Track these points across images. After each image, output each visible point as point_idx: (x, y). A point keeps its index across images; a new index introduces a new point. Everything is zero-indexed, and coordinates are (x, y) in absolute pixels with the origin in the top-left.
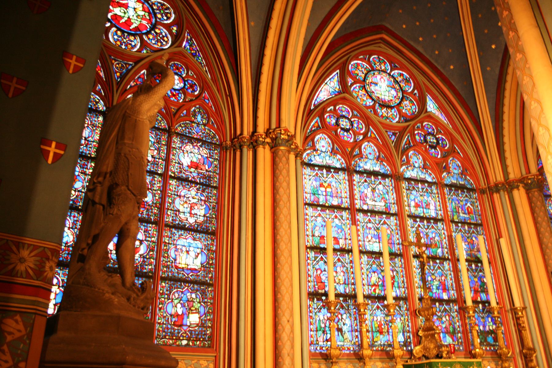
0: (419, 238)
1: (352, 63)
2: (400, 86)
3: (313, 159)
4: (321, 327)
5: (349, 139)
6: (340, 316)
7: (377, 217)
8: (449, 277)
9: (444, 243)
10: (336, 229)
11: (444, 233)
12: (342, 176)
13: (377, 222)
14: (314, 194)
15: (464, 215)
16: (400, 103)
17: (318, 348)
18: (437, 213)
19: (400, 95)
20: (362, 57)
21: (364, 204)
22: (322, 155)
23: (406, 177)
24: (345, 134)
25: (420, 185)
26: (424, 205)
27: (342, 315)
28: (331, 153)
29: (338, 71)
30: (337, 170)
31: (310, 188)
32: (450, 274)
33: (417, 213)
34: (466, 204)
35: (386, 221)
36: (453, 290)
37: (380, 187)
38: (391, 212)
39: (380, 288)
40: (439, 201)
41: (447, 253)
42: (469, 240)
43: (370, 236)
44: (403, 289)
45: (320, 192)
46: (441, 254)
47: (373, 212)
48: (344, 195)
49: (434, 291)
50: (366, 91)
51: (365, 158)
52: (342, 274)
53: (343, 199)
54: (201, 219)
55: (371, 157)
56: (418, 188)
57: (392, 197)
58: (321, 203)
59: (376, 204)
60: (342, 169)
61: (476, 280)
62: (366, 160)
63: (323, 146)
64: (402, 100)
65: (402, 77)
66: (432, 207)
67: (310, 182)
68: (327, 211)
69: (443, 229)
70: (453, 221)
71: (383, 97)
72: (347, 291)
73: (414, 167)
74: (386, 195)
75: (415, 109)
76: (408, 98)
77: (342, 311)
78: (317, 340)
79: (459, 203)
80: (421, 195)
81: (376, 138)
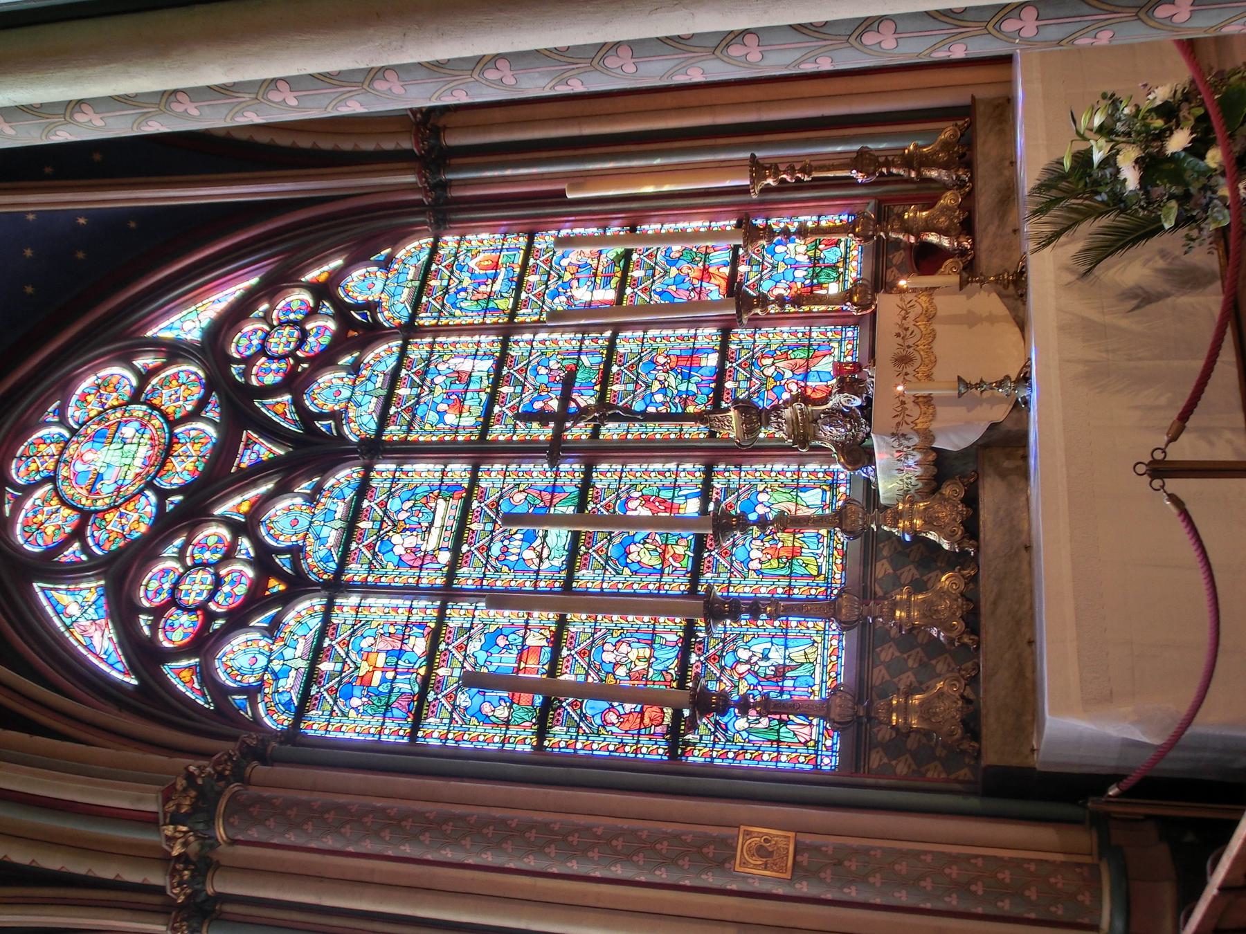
0: (542, 417)
1: (21, 540)
2: (114, 408)
3: (286, 698)
4: (769, 728)
5: (243, 580)
6: (742, 668)
7: (474, 527)
9: (568, 346)
10: (495, 650)
13: (489, 527)
14: (388, 706)
15: (499, 281)
17: (829, 743)
18: (485, 354)
19: (139, 410)
20: (7, 509)
22: (277, 669)
23: (373, 426)
24: (226, 589)
26: (459, 387)
27: (738, 662)
29: (36, 586)
31: (367, 718)
33: (478, 411)
34: (471, 271)
35: (488, 502)
36: (695, 336)
41: (595, 340)
42: (567, 277)
43: (529, 554)
44: (682, 474)
45: (384, 688)
46: (597, 359)
48: (401, 618)
49: (693, 388)
50: (113, 507)
51: (304, 538)
52: (624, 648)
53: (413, 619)
56: (408, 398)
58: (416, 689)
61: (674, 271)
62: (311, 539)
65: (89, 398)
66: (466, 365)
67: (352, 714)
68: (442, 672)
69: (531, 342)
70: (513, 313)
71: (138, 462)
72: (673, 638)
74: (418, 491)
75: (189, 371)
76: (154, 390)
77: (729, 660)
78: (805, 744)
79: (465, 290)
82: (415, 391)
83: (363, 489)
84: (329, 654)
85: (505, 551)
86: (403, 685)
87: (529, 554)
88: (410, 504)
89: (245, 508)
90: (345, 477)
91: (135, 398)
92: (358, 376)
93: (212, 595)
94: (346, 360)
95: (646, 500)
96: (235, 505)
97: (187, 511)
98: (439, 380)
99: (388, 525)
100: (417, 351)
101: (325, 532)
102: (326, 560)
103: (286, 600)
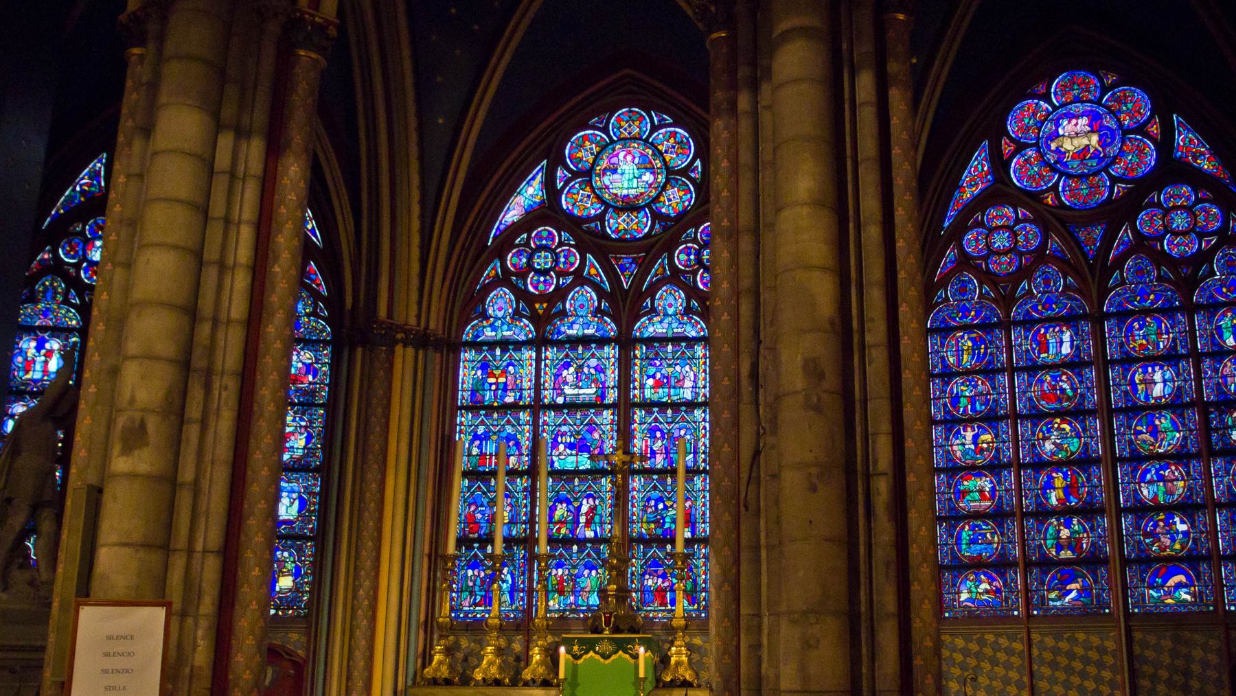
2: (664, 160)
8: (699, 503)
11: (704, 428)
12: (528, 354)
13: (578, 422)
16: (659, 195)
21: (559, 395)
24: (542, 279)
25: (670, 348)
28: (512, 318)
30: (518, 345)
32: (704, 497)
33: (655, 398)
36: (704, 522)
37: (593, 362)
38: (606, 402)
39: (569, 526)
40: (705, 371)
41: (704, 461)
47: (572, 406)
48: (526, 385)
49: (667, 526)
50: (593, 190)
52: (509, 508)
54: (300, 452)
55: (581, 312)
57: (612, 377)
59: (581, 391)
60: (527, 343)
63: (500, 309)
64: (664, 188)
65: (672, 140)
66: (688, 383)
68: (495, 415)
71: (625, 192)
73: (666, 315)
76: (677, 180)
80: (670, 366)
81: (598, 275)
82: (670, 356)
83: (602, 342)
84: (504, 351)
85: (564, 434)
86: (488, 396)
87: (561, 447)
88: (593, 371)
89: (593, 271)
90: (611, 328)
91: (670, 171)
92: (682, 315)
93: (539, 272)
94: (694, 303)
95: (592, 510)
96: (594, 268)
97: (589, 236)
98: (678, 368)
99: (580, 362)
100: (699, 350)
101: (576, 326)
102: (559, 333)
103: (534, 318)
